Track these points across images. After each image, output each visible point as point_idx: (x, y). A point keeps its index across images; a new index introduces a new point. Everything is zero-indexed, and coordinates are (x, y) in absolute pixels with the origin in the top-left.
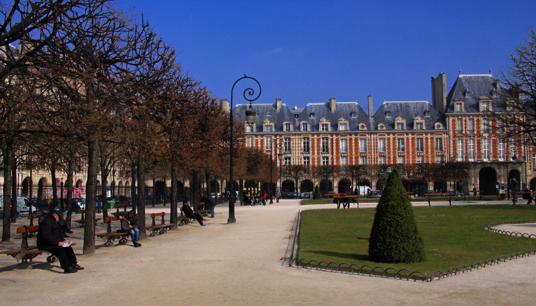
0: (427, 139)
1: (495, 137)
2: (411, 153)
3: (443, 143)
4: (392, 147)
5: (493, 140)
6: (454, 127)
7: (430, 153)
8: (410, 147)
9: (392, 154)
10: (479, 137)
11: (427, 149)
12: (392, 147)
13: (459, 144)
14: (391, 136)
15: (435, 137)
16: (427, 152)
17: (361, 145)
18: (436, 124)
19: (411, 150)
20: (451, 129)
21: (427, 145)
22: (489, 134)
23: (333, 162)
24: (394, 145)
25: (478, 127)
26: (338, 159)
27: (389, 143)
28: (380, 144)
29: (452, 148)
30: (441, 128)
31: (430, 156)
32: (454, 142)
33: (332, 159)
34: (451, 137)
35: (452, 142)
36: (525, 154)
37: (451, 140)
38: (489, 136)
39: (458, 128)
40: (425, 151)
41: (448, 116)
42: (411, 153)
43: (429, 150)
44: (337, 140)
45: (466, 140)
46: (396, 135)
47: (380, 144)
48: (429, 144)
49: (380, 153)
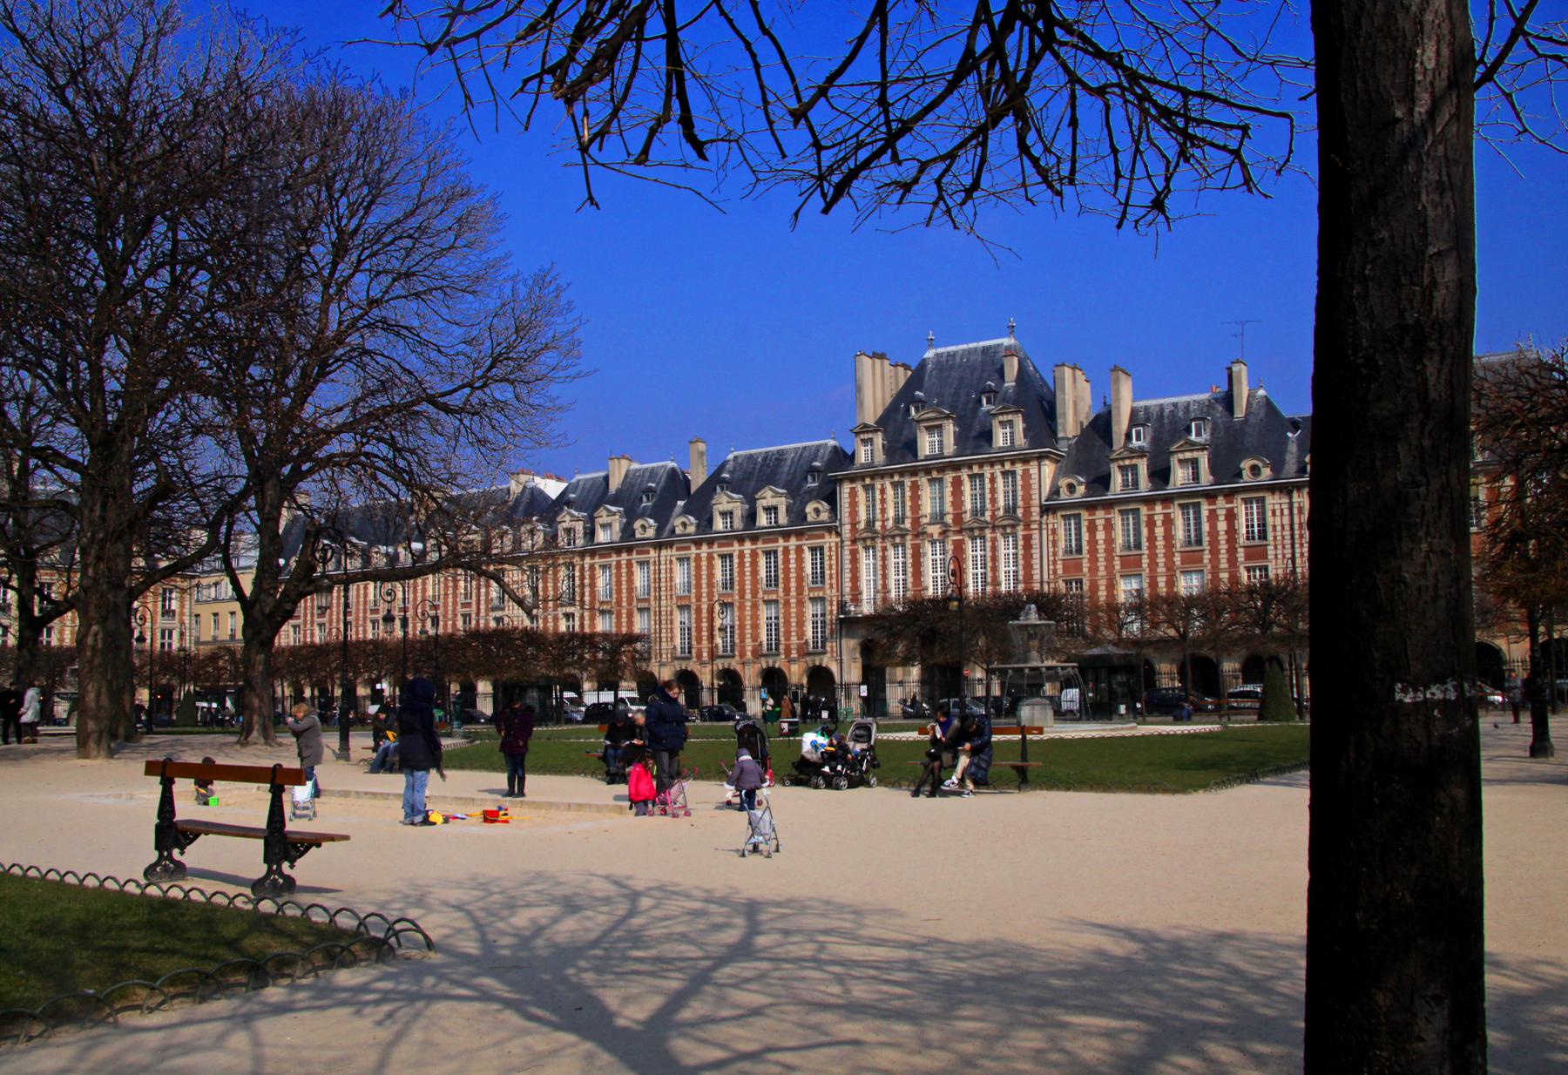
0: (786, 551)
1: (959, 532)
2: (748, 596)
3: (827, 563)
4: (704, 581)
5: (954, 542)
6: (854, 513)
7: (793, 593)
8: (748, 578)
9: (705, 599)
10: (916, 536)
11: (787, 580)
12: (704, 581)
13: (866, 562)
14: (705, 548)
15: (806, 543)
16: (787, 590)
17: (640, 579)
18: (809, 508)
19: (748, 587)
20: (846, 518)
21: (787, 571)
22: (945, 525)
23: (582, 625)
24: (711, 576)
25: (916, 507)
26: (592, 619)
27: (698, 568)
28: (680, 575)
29: (847, 576)
30: (824, 516)
31: (793, 601)
32: (854, 553)
33: (582, 617)
34: (847, 543)
35: (847, 557)
36: (1042, 583)
37: (847, 552)
38: (944, 533)
39: (862, 516)
40: (781, 585)
41: (841, 481)
42: (748, 596)
43: (793, 584)
44: (592, 567)
45: (884, 549)
46: (715, 548)
47: (680, 575)
48: (793, 566)
49: (679, 598)
